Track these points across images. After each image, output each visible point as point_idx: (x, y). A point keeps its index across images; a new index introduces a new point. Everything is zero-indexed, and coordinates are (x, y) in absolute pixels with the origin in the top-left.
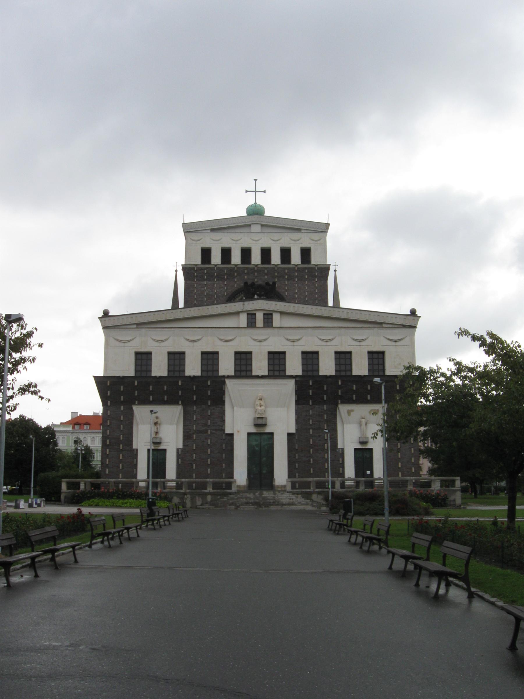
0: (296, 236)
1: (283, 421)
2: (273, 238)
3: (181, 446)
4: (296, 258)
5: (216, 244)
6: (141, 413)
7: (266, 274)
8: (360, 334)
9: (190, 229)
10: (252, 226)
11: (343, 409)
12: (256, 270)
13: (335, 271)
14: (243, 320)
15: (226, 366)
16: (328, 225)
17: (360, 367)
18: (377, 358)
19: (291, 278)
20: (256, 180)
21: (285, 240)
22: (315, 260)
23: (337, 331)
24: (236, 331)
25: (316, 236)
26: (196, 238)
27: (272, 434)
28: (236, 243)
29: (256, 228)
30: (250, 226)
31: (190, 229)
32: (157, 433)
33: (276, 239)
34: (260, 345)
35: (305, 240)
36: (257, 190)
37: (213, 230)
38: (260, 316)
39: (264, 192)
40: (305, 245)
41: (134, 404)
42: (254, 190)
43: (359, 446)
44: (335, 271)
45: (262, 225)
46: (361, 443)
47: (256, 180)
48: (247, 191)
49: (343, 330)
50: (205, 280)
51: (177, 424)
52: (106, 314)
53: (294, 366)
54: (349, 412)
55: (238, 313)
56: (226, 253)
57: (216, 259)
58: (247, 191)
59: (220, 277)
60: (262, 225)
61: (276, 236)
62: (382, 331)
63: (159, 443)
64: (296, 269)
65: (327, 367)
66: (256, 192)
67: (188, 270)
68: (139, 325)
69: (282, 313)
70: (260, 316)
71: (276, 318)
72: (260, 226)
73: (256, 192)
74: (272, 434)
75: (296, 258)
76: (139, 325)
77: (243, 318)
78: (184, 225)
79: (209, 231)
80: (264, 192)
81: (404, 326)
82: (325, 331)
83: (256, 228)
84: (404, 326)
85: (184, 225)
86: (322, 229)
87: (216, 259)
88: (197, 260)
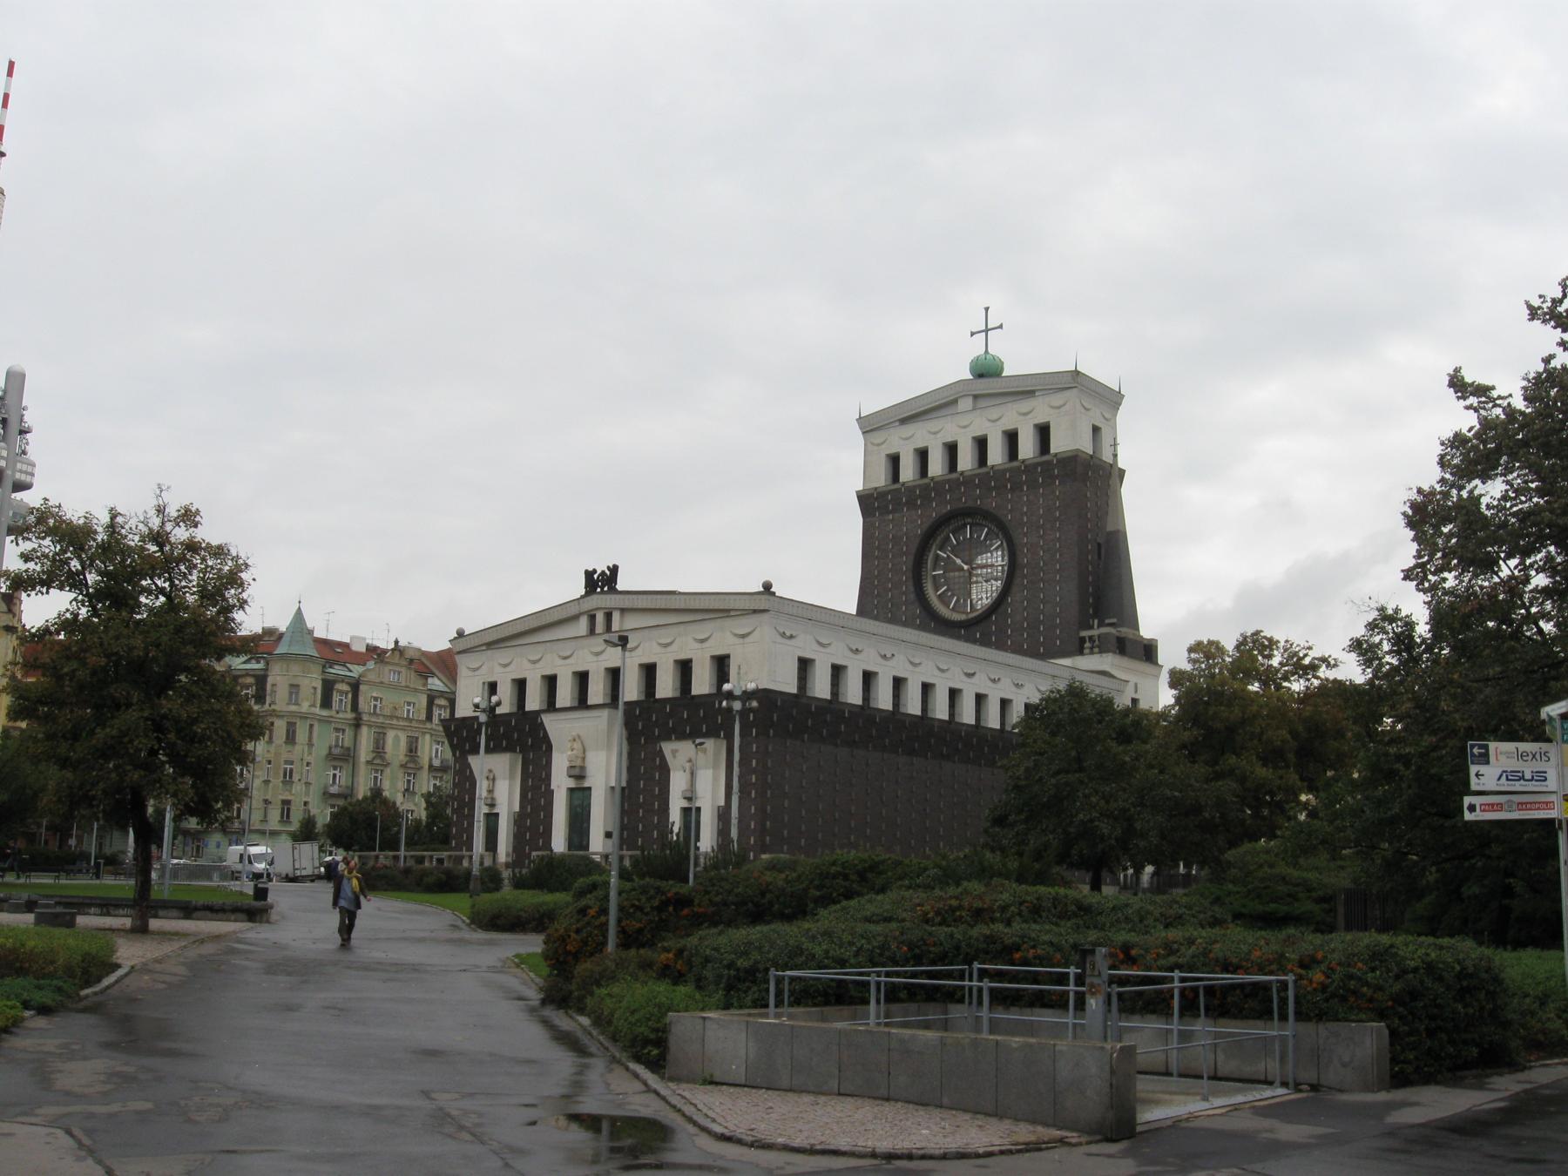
0: (1024, 406)
1: (605, 770)
3: (517, 809)
4: (1027, 448)
5: (905, 443)
6: (678, 753)
7: (978, 486)
8: (702, 630)
9: (871, 426)
11: (667, 748)
12: (967, 480)
13: (1115, 456)
14: (582, 626)
15: (565, 695)
17: (702, 684)
18: (721, 664)
19: (1017, 487)
20: (987, 309)
22: (1058, 445)
23: (674, 630)
24: (573, 643)
25: (1057, 399)
27: (589, 789)
28: (932, 436)
29: (965, 404)
31: (871, 426)
32: (490, 791)
33: (995, 417)
34: (597, 659)
35: (1041, 410)
37: (903, 421)
38: (600, 618)
40: (1041, 420)
41: (475, 751)
43: (685, 804)
45: (976, 397)
46: (689, 799)
49: (682, 627)
50: (889, 512)
51: (512, 777)
52: (460, 634)
53: (631, 690)
54: (674, 752)
55: (576, 618)
56: (923, 455)
57: (908, 473)
59: (911, 504)
60: (976, 397)
61: (994, 413)
62: (728, 623)
63: (492, 805)
64: (1029, 468)
65: (666, 687)
66: (987, 331)
67: (869, 502)
68: (490, 645)
69: (623, 611)
70: (600, 618)
71: (616, 616)
72: (970, 400)
74: (589, 789)
75: (1027, 448)
76: (490, 645)
77: (584, 621)
78: (861, 420)
81: (755, 611)
82: (662, 631)
83: (965, 404)
84: (755, 611)
87: (908, 473)
88: (881, 480)
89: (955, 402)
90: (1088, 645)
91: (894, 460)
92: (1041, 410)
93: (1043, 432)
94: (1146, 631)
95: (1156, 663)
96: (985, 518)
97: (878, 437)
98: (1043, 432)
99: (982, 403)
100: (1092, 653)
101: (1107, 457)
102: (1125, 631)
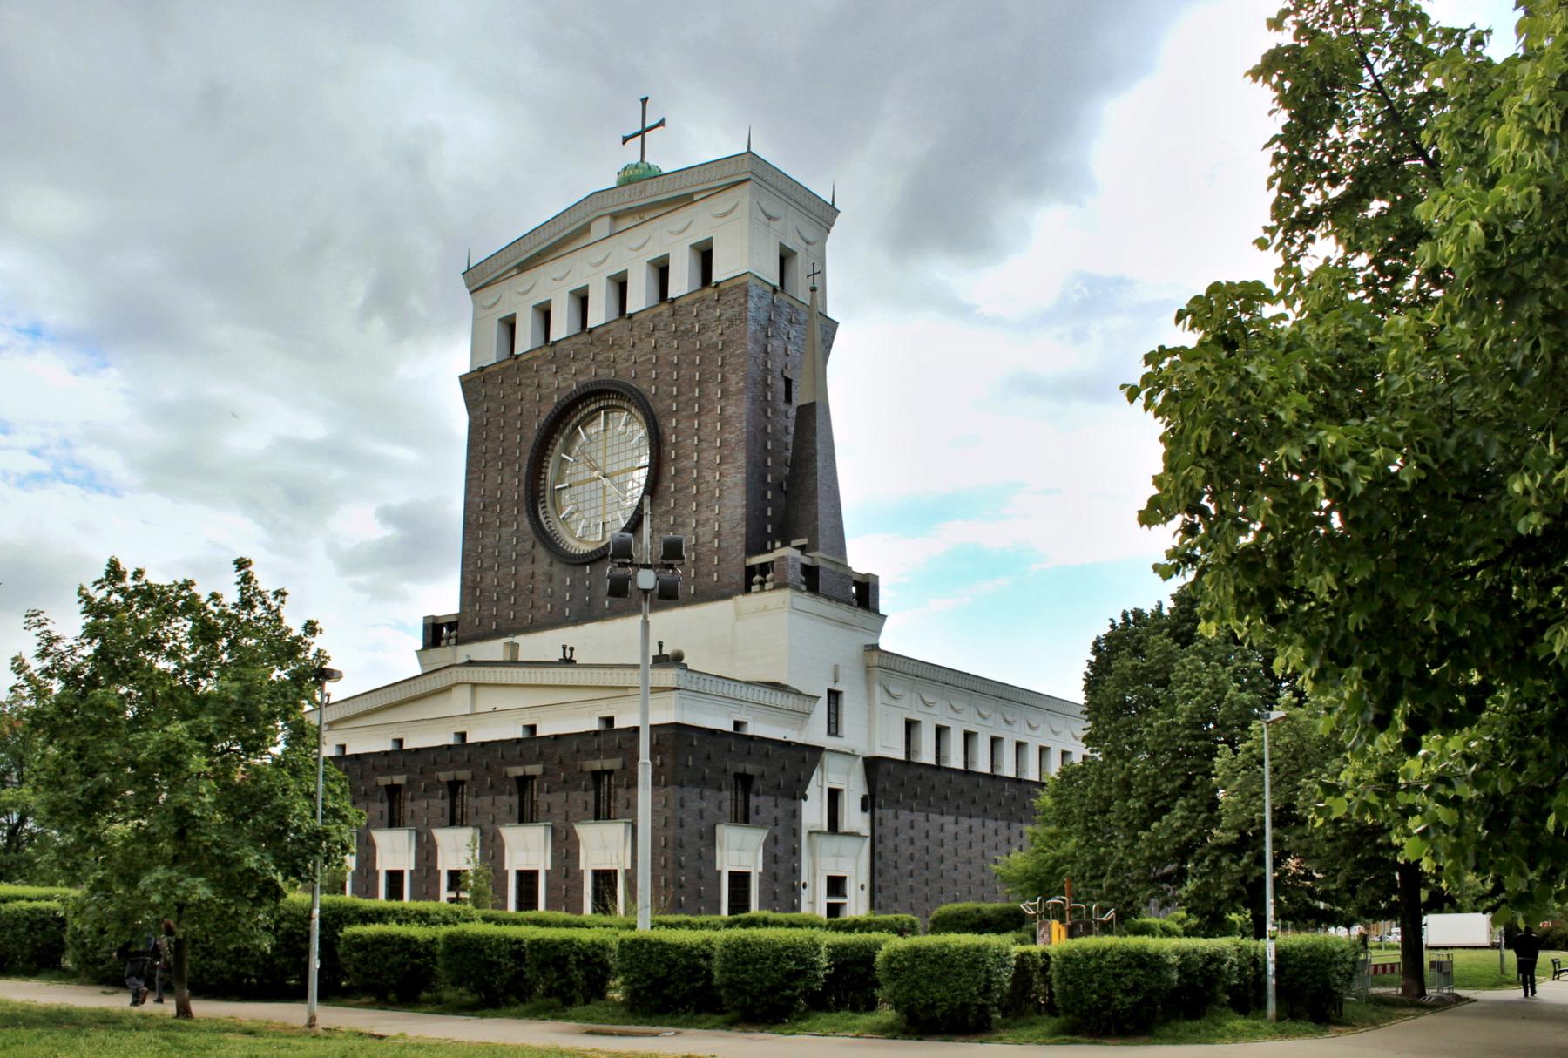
25: (722, 202)
26: (490, 302)
31: (480, 279)
37: (523, 267)
60: (615, 217)
75: (681, 283)
83: (600, 228)
89: (585, 229)
90: (757, 578)
91: (510, 325)
92: (697, 223)
93: (705, 255)
94: (859, 561)
95: (877, 611)
96: (620, 396)
97: (489, 295)
98: (705, 255)
99: (625, 223)
100: (762, 590)
101: (803, 295)
102: (818, 557)
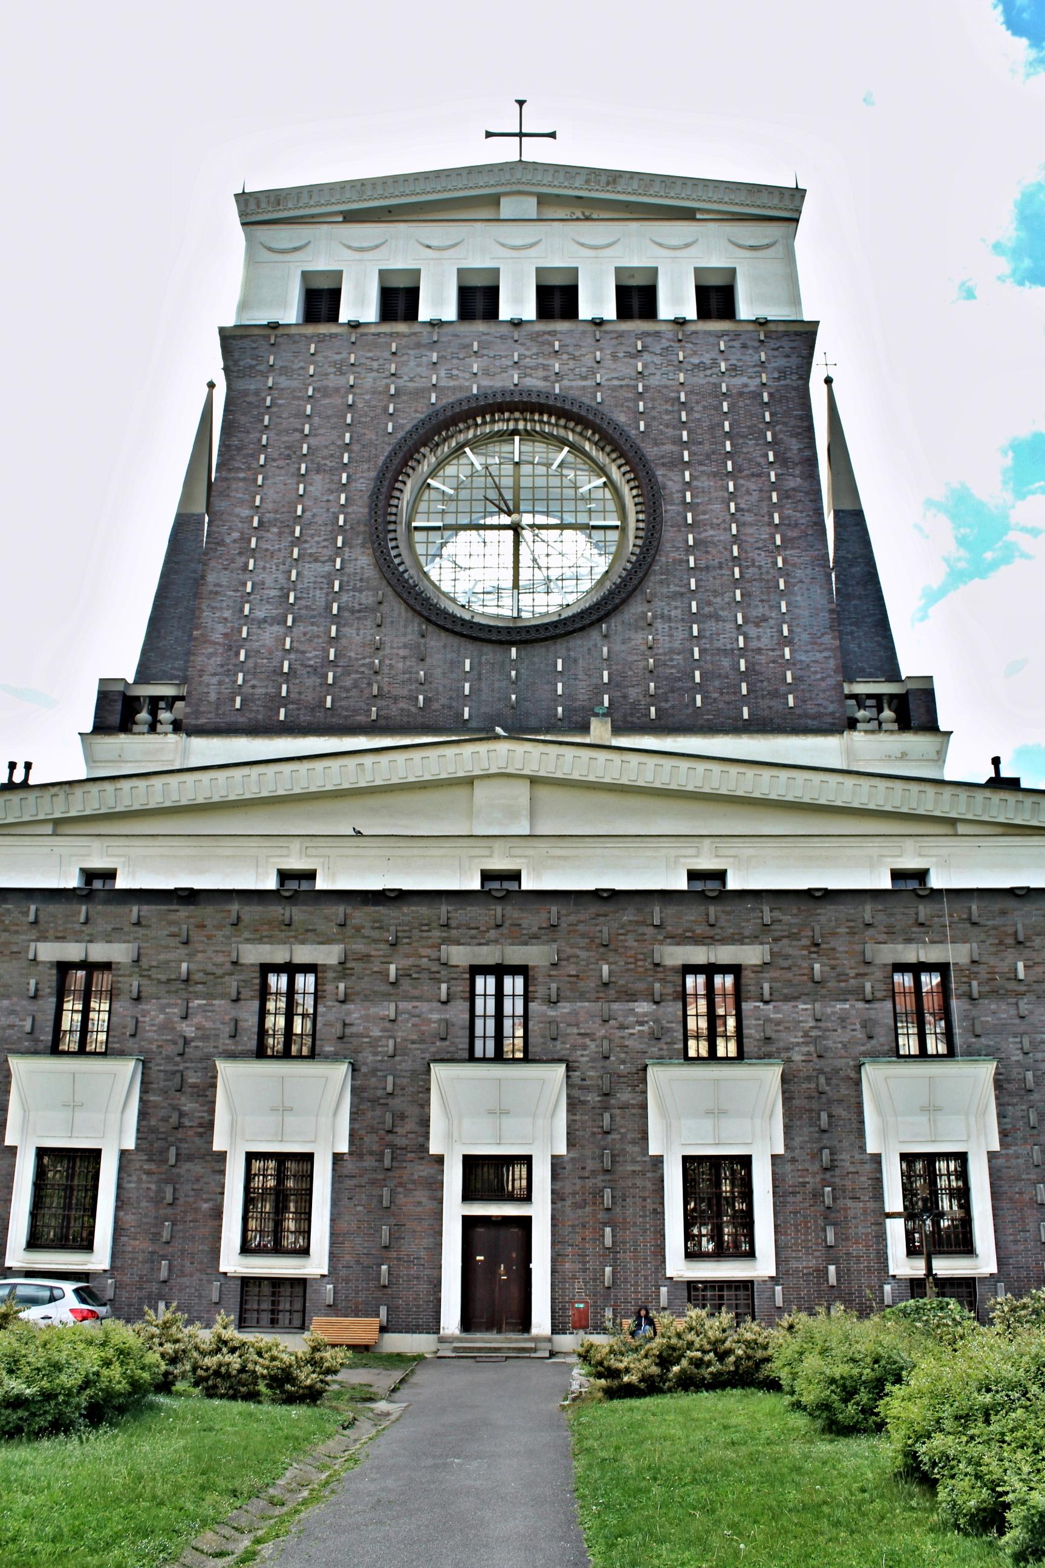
2: (583, 241)
10: (503, 200)
13: (828, 381)
16: (798, 194)
20: (521, 103)
21: (637, 247)
30: (494, 201)
36: (524, 131)
37: (351, 217)
39: (553, 135)
42: (518, 131)
44: (828, 381)
47: (521, 103)
48: (489, 135)
58: (489, 135)
66: (521, 135)
72: (534, 200)
73: (521, 135)
78: (243, 199)
79: (341, 219)
80: (553, 135)
85: (243, 199)
86: (776, 210)
